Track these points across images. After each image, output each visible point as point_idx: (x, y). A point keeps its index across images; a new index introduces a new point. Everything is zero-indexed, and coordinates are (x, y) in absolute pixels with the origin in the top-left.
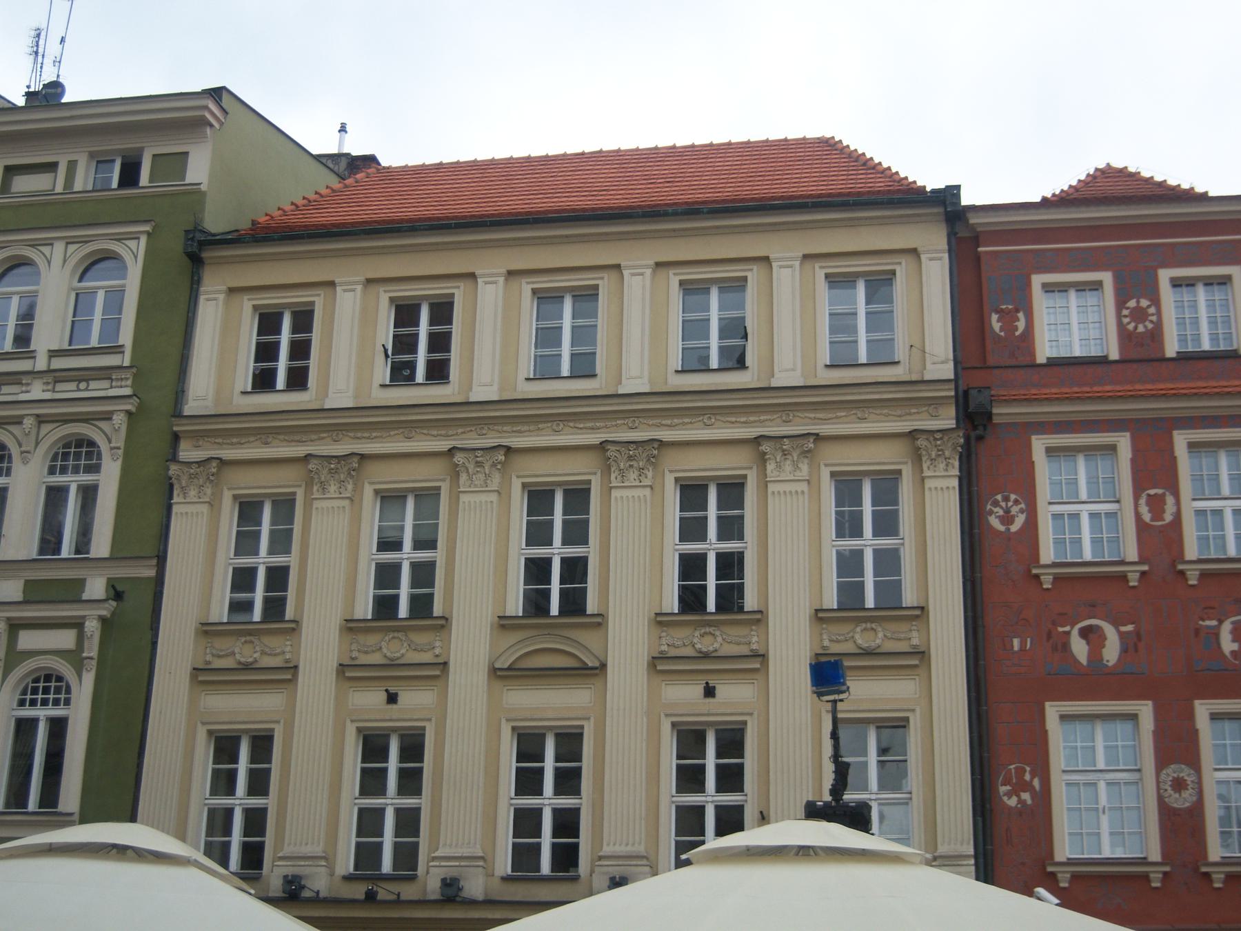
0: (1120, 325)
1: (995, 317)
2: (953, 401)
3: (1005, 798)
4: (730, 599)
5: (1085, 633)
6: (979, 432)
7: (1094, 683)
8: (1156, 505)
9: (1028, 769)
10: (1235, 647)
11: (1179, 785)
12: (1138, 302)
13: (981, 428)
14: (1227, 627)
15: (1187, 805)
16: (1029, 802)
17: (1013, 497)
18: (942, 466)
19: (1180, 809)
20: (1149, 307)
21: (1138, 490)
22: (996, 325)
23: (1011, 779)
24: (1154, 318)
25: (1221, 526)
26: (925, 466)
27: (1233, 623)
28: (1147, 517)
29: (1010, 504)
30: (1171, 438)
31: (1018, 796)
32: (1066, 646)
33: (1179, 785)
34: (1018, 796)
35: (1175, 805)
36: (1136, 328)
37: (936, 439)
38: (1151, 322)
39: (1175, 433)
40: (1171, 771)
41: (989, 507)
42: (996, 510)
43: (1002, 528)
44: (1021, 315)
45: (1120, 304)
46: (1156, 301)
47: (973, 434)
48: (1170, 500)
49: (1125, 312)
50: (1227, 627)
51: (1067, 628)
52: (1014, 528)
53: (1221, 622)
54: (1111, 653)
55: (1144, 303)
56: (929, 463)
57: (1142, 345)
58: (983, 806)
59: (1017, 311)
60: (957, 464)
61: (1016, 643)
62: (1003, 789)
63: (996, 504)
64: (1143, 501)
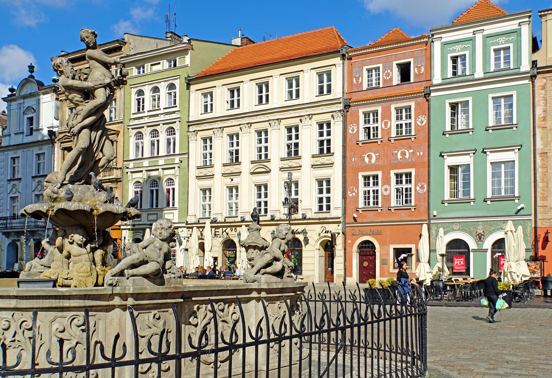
1: (354, 79)
4: (296, 152)
5: (368, 156)
8: (386, 124)
10: (401, 157)
11: (386, 190)
14: (400, 152)
22: (355, 81)
28: (384, 127)
32: (364, 159)
44: (360, 78)
45: (384, 72)
46: (392, 70)
48: (389, 122)
50: (400, 152)
52: (354, 132)
54: (373, 160)
61: (353, 159)
62: (349, 192)
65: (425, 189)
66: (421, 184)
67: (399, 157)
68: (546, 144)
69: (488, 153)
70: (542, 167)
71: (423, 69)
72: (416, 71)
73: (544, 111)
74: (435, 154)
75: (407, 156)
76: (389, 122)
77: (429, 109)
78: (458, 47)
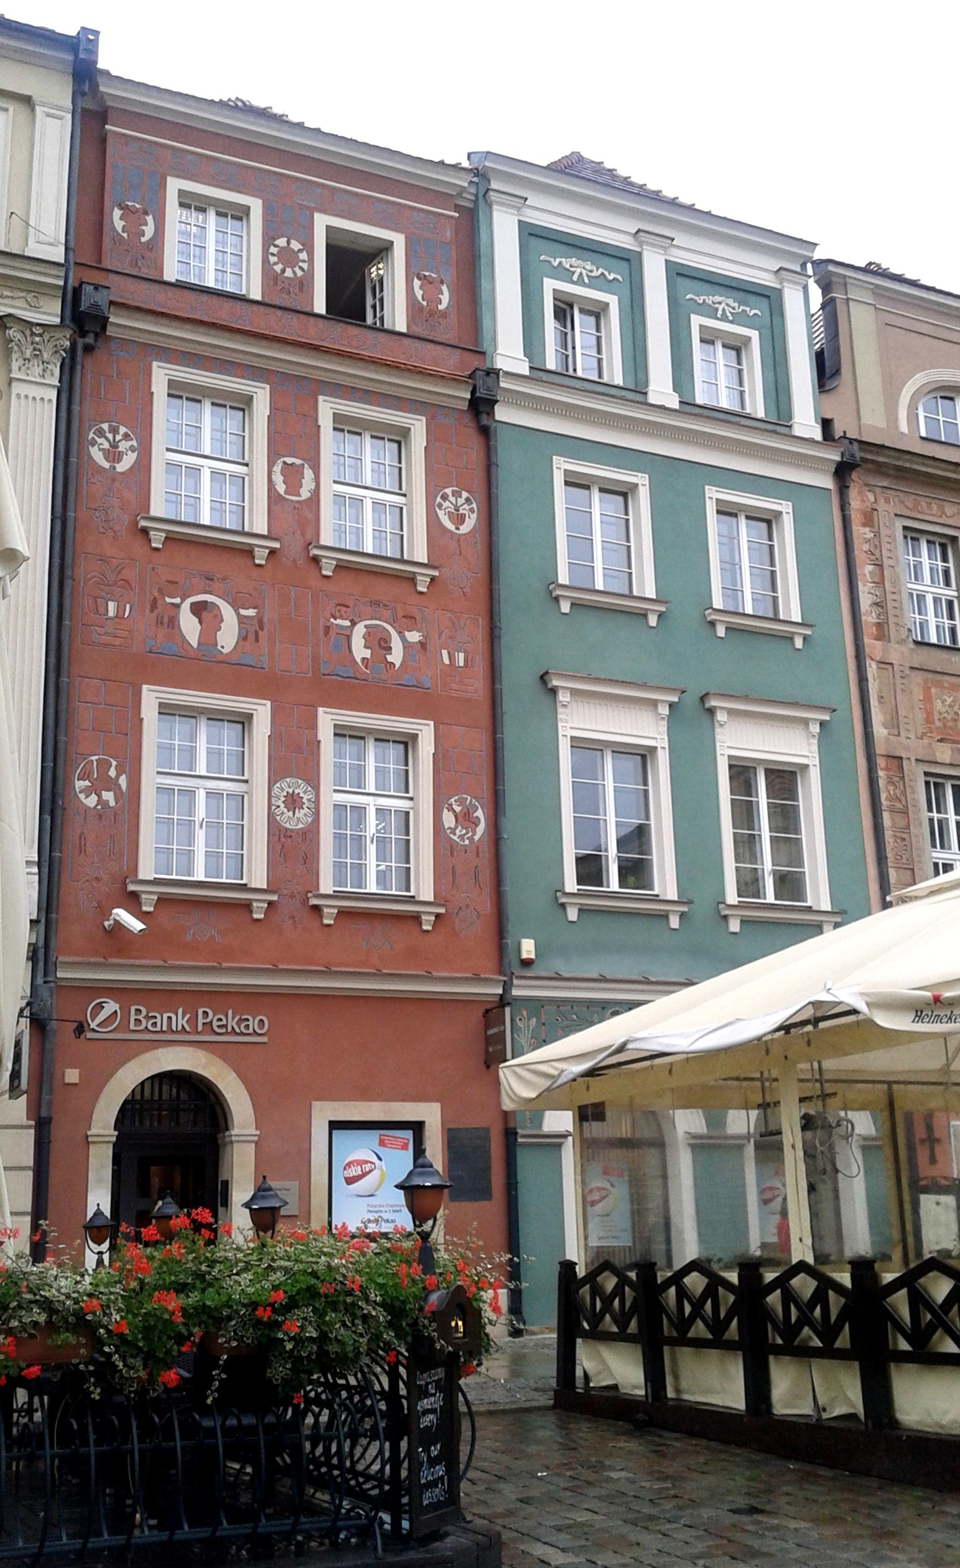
0: (265, 261)
1: (117, 213)
2: (60, 294)
3: (82, 796)
5: (198, 609)
6: (89, 339)
7: (203, 668)
8: (293, 476)
9: (114, 763)
10: (367, 653)
12: (288, 243)
13: (92, 335)
14: (359, 630)
15: (300, 826)
16: (112, 803)
17: (123, 430)
18: (38, 370)
19: (292, 831)
20: (300, 251)
21: (273, 455)
22: (119, 224)
23: (91, 772)
24: (305, 266)
25: (359, 518)
26: (15, 365)
27: (366, 626)
28: (281, 488)
29: (118, 437)
30: (316, 401)
31: (99, 796)
32: (173, 622)
33: (293, 802)
34: (99, 796)
35: (287, 825)
36: (283, 271)
37: (33, 334)
38: (301, 269)
39: (321, 398)
40: (286, 786)
41: (91, 435)
42: (99, 441)
43: (106, 465)
44: (150, 219)
45: (268, 240)
47: (81, 342)
48: (308, 473)
49: (273, 250)
50: (359, 630)
51: (177, 600)
52: (122, 467)
53: (354, 623)
54: (227, 638)
55: (295, 245)
56: (21, 362)
57: (289, 293)
58: (54, 802)
59: (146, 213)
60: (57, 372)
61: (112, 606)
62: (80, 784)
63: (101, 433)
64: (277, 468)
65: (481, 829)
66: (461, 802)
67: (360, 651)
68: (894, 723)
69: (721, 716)
70: (892, 811)
71: (445, 298)
72: (419, 294)
73: (876, 604)
74: (517, 673)
75: (396, 657)
76: (308, 473)
77: (489, 466)
78: (582, 266)
